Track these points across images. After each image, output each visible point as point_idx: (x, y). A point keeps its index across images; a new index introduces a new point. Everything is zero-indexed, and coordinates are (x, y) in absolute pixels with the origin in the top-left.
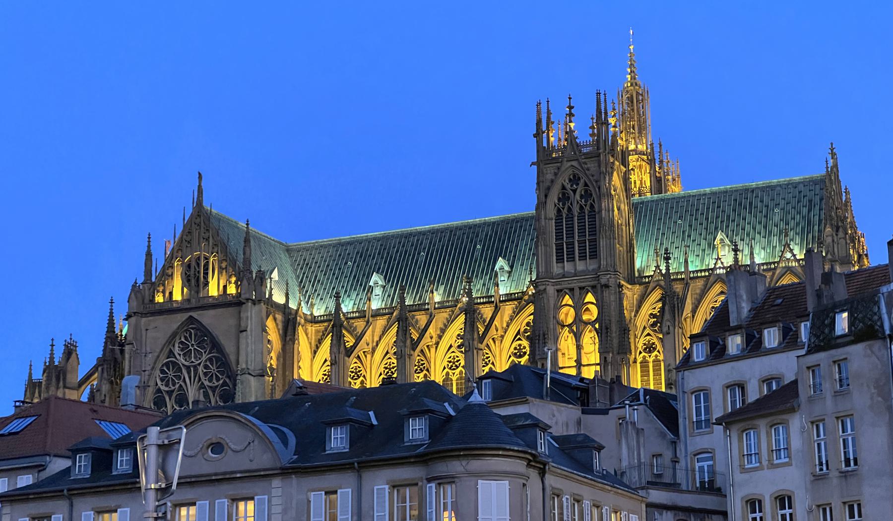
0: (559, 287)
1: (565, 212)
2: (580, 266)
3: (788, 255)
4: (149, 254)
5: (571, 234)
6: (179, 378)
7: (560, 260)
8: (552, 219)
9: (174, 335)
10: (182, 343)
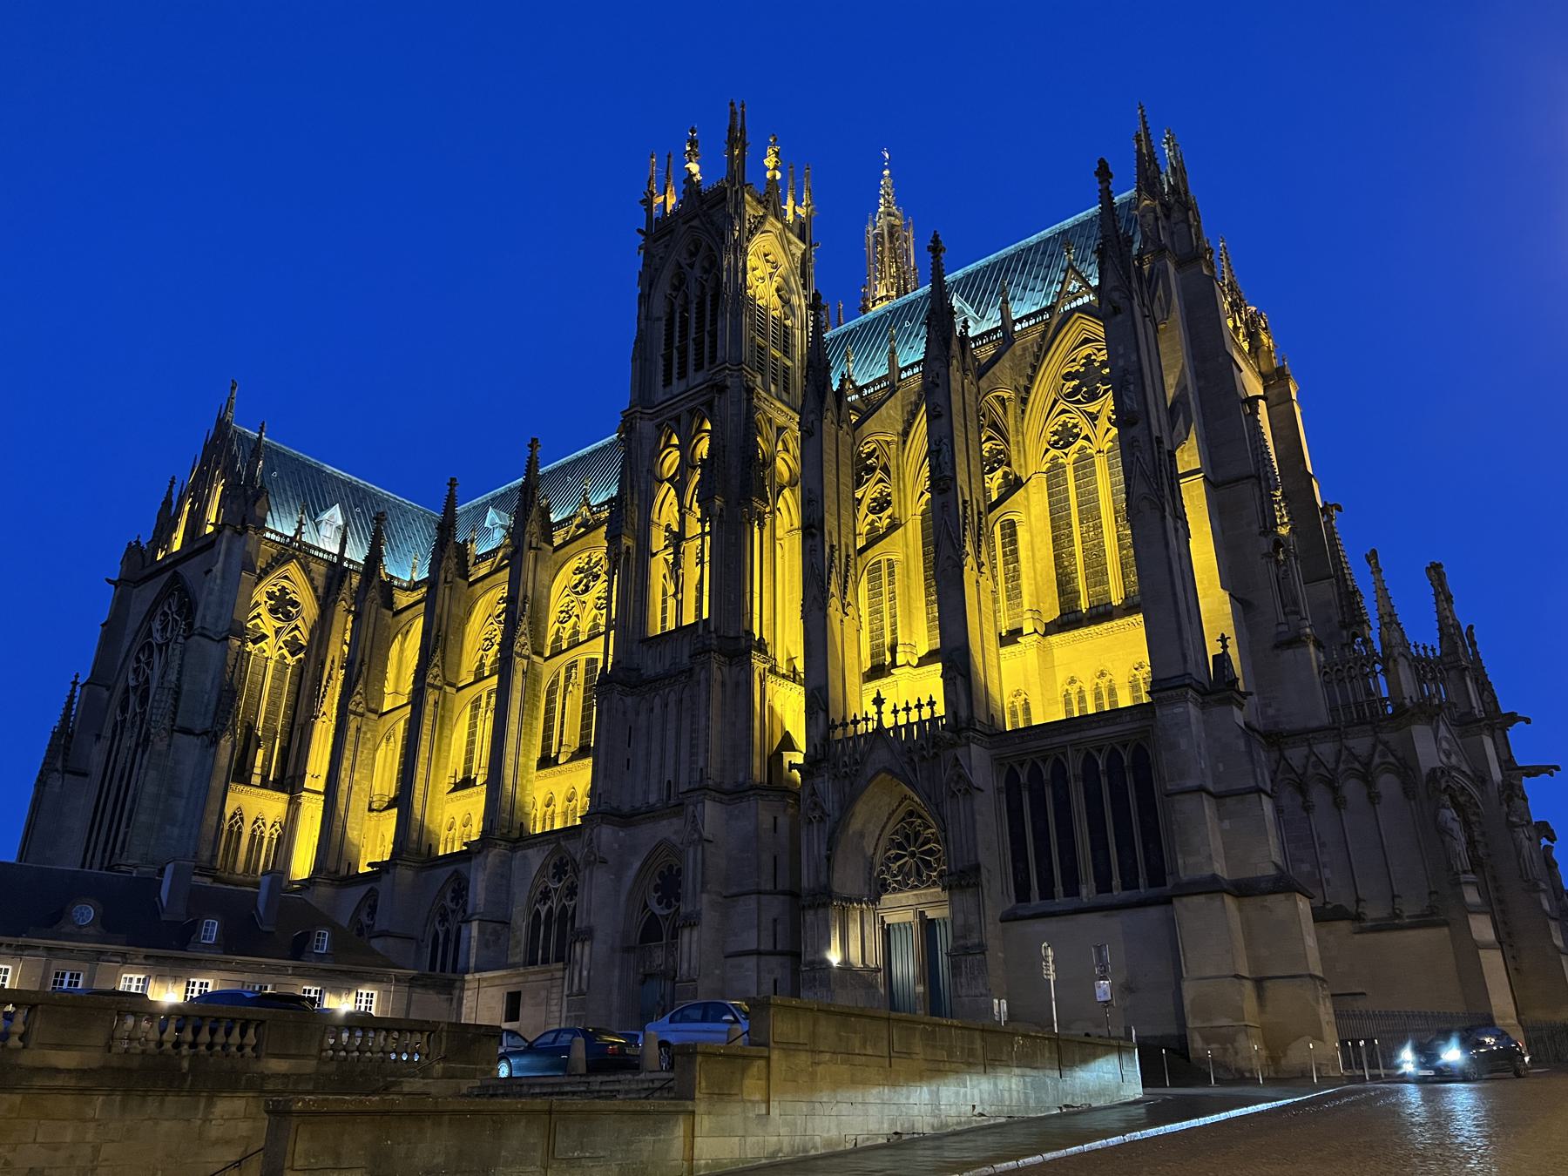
2: (695, 378)
3: (1074, 285)
5: (684, 336)
6: (148, 664)
7: (668, 382)
8: (659, 319)
9: (156, 604)
10: (164, 614)
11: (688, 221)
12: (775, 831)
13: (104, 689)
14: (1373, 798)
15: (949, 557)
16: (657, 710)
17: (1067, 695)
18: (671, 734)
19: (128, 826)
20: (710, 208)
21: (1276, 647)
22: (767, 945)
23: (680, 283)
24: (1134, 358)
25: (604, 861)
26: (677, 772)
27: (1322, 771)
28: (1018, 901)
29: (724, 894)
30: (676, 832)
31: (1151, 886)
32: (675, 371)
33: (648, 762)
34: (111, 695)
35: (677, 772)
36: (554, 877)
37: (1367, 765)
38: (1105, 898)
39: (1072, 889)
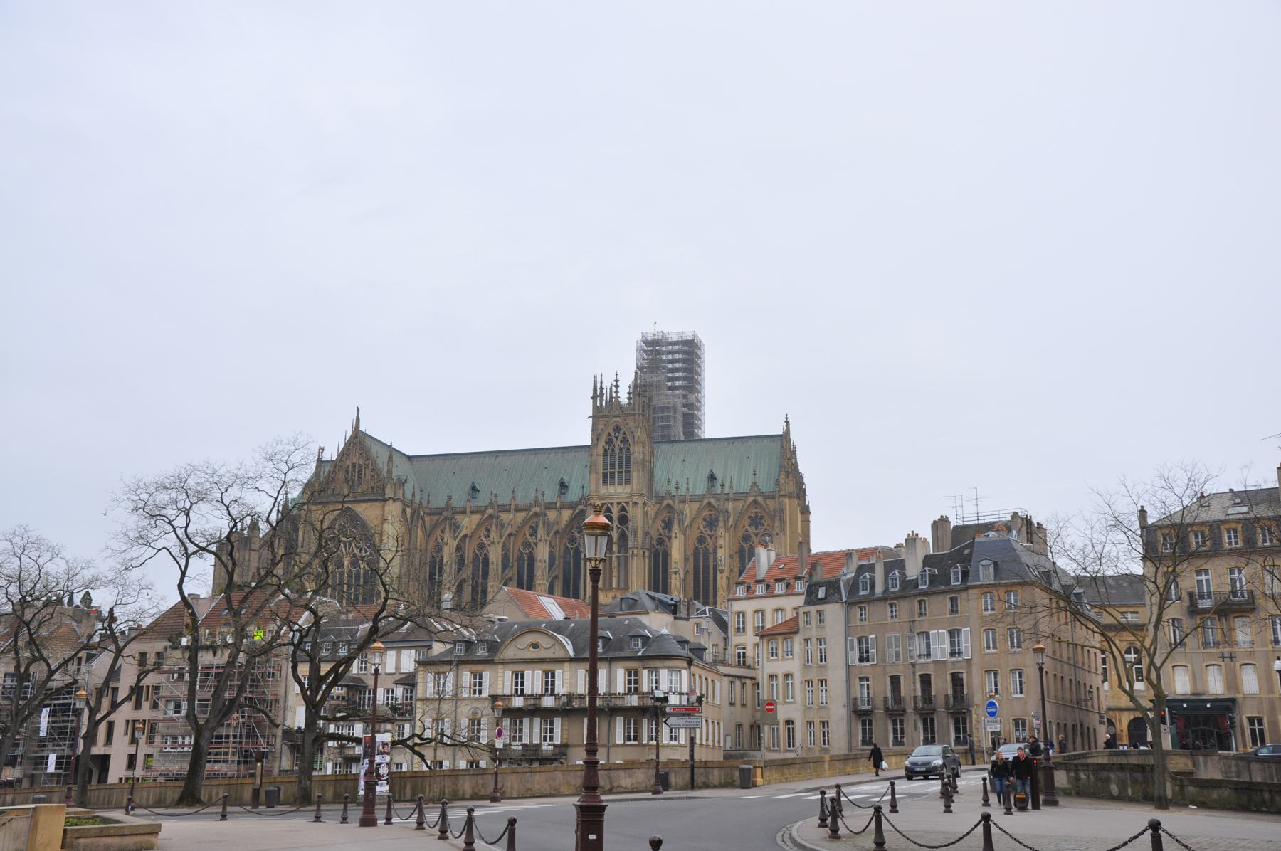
7: (605, 483)
23: (609, 441)
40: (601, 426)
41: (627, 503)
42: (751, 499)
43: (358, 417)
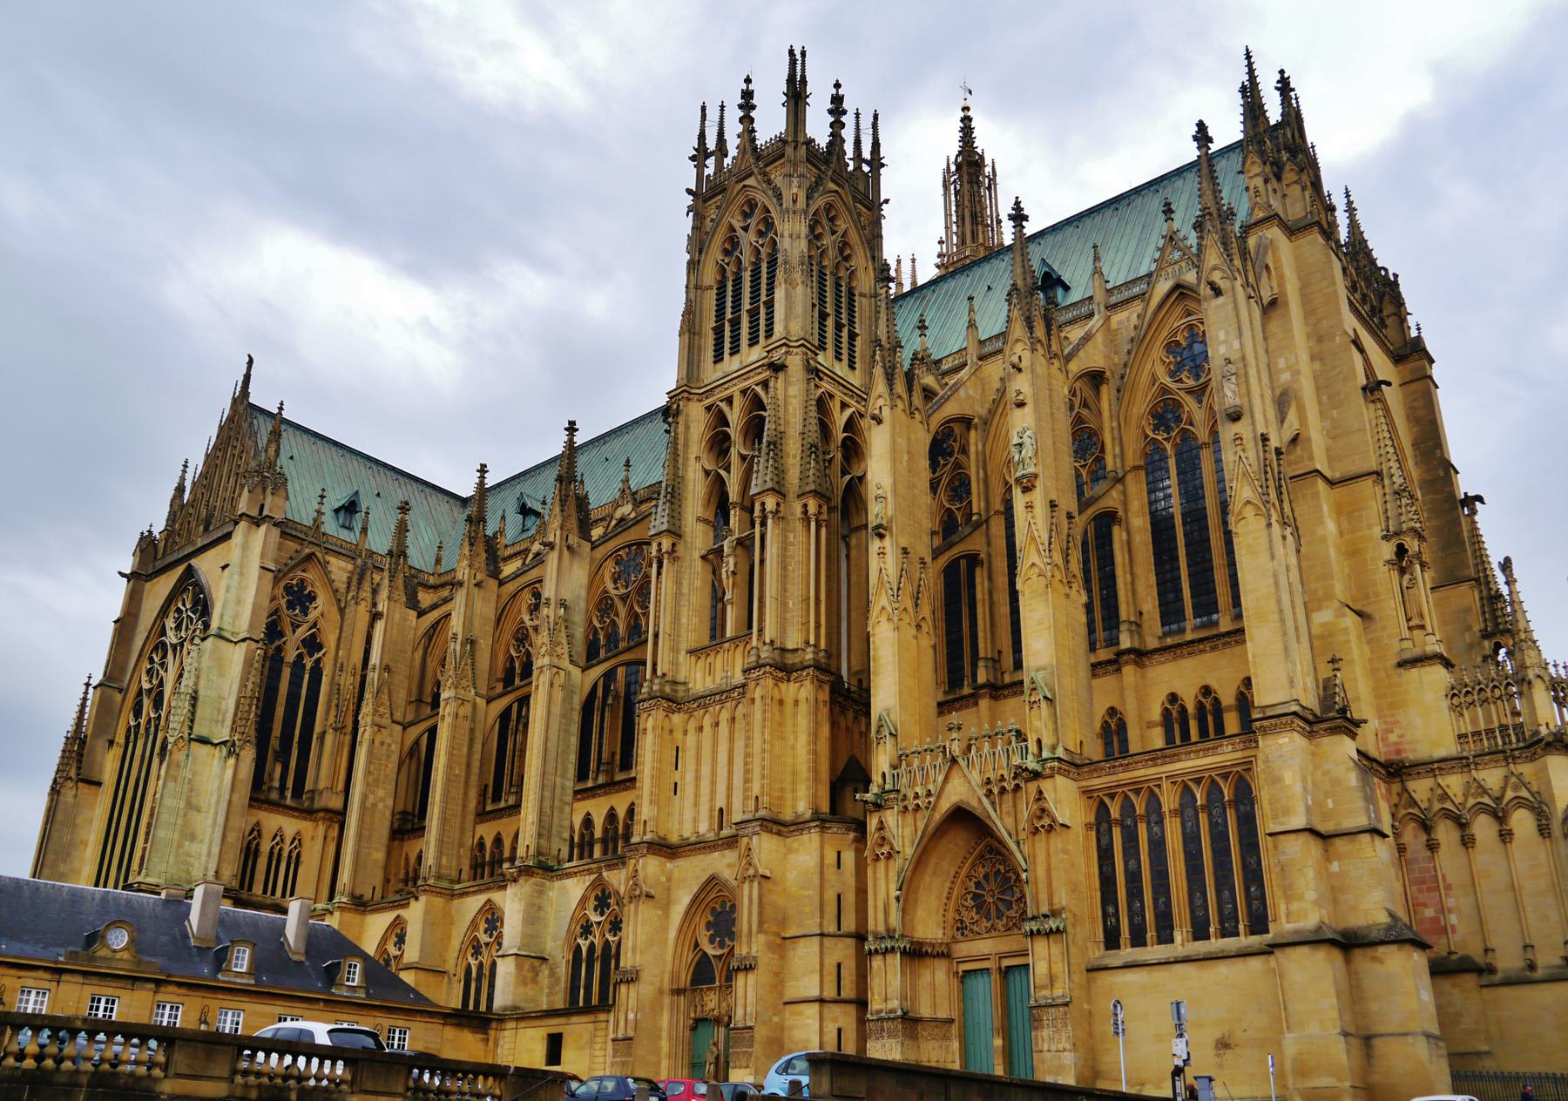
0: (708, 402)
1: (730, 270)
4: (180, 489)
6: (162, 665)
7: (718, 358)
8: (710, 288)
10: (178, 611)
11: (741, 181)
12: (839, 867)
13: (116, 692)
14: (1506, 836)
15: (1033, 564)
16: (707, 729)
17: (1166, 714)
18: (722, 756)
19: (146, 841)
20: (767, 165)
21: (1401, 665)
22: (830, 993)
23: (733, 243)
24: (1236, 345)
25: (649, 896)
26: (729, 796)
27: (1448, 805)
28: (1108, 948)
29: (783, 935)
30: (729, 866)
31: (1252, 933)
32: (727, 345)
33: (697, 787)
34: (124, 699)
35: (729, 796)
36: (595, 910)
37: (1498, 799)
38: (1201, 947)
39: (1165, 937)
40: (712, 213)
41: (765, 384)
42: (1163, 287)
43: (247, 377)
